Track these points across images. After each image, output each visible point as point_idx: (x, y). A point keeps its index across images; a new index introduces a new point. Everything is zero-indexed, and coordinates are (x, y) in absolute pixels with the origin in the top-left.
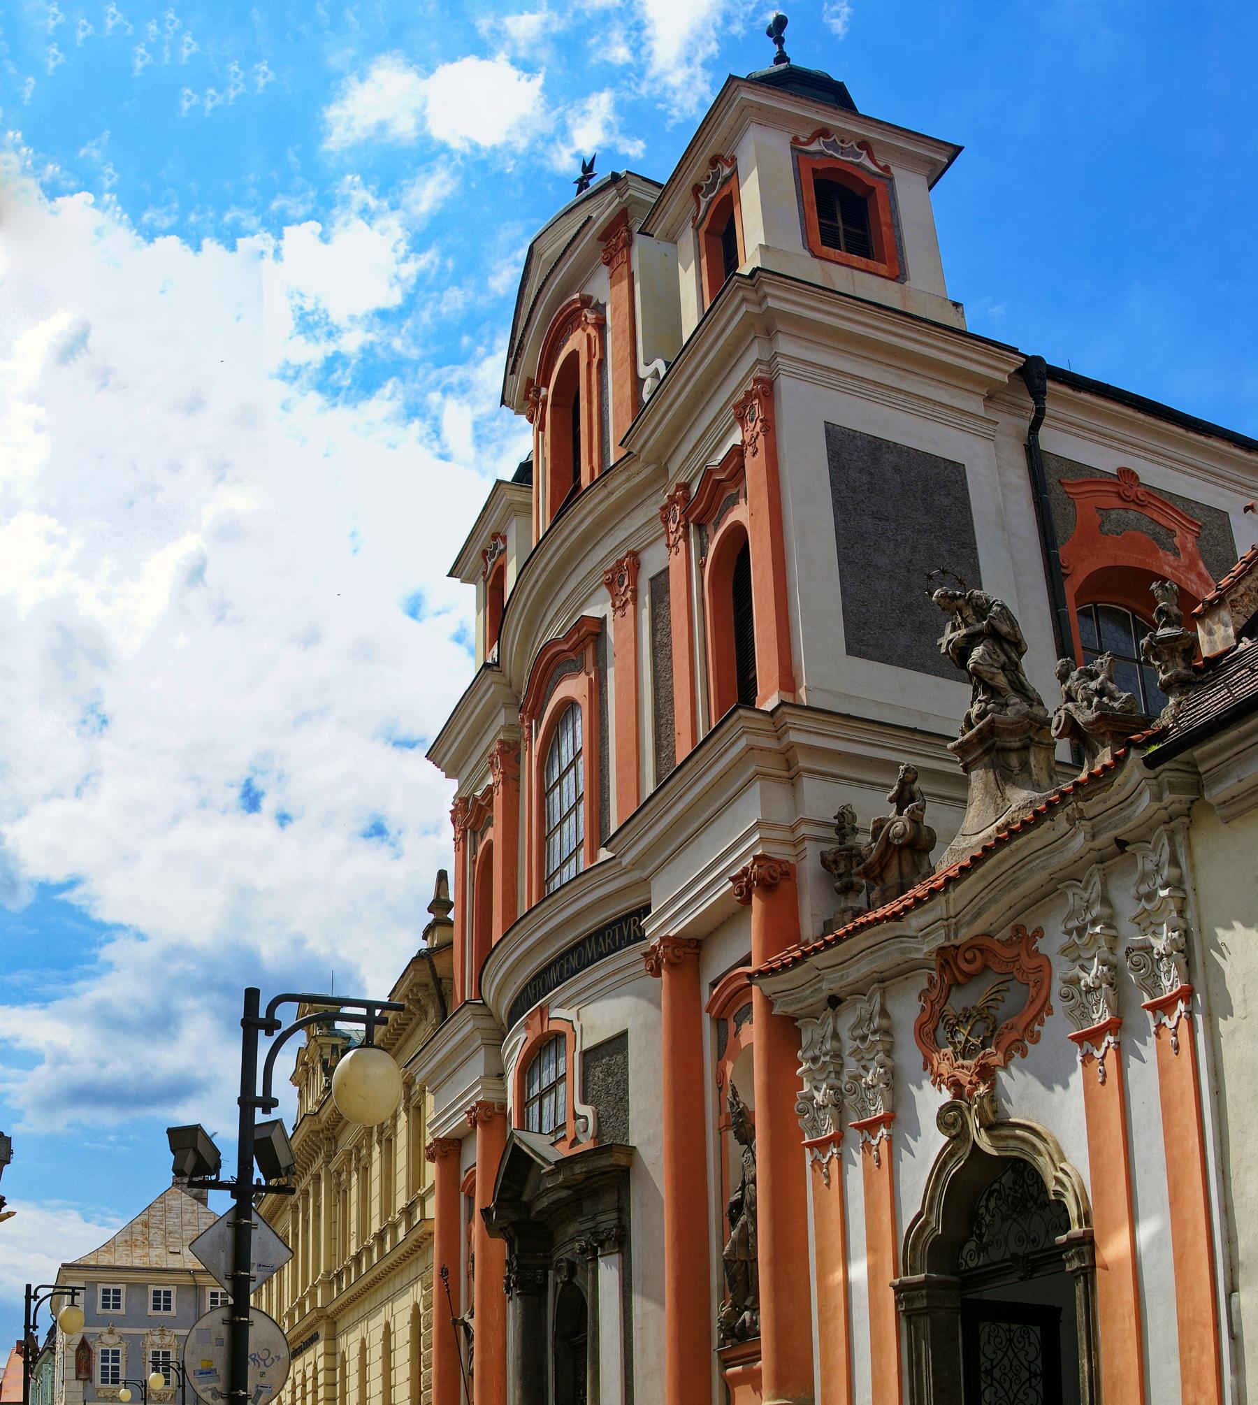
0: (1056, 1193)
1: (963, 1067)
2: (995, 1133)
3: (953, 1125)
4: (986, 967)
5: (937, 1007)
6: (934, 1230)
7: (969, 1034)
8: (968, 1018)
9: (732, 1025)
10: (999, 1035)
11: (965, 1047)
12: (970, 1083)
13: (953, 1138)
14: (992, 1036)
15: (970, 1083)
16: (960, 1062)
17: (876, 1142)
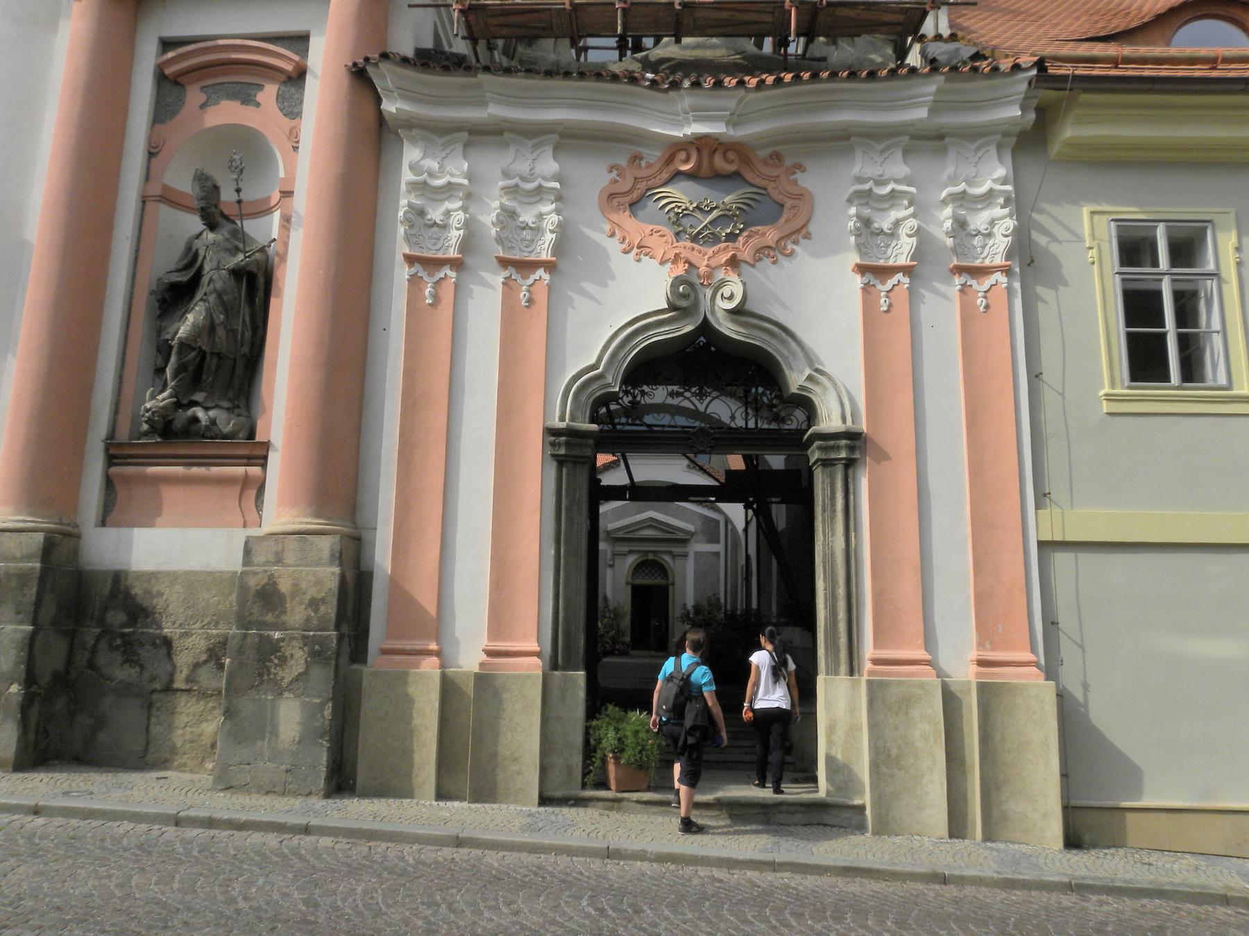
0: (802, 388)
1: (693, 249)
2: (743, 319)
3: (685, 296)
4: (736, 175)
5: (642, 186)
6: (609, 385)
7: (710, 223)
8: (713, 209)
9: (194, 96)
10: (749, 237)
11: (699, 233)
12: (707, 266)
13: (672, 307)
14: (737, 235)
15: (707, 266)
16: (689, 244)
17: (530, 281)
